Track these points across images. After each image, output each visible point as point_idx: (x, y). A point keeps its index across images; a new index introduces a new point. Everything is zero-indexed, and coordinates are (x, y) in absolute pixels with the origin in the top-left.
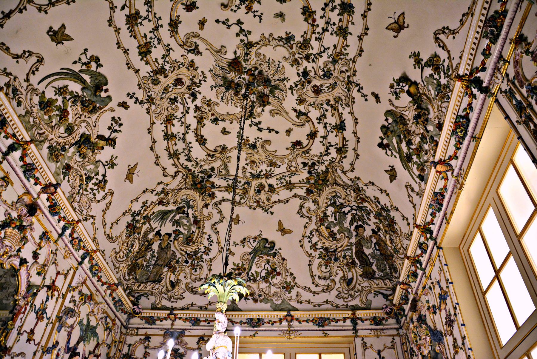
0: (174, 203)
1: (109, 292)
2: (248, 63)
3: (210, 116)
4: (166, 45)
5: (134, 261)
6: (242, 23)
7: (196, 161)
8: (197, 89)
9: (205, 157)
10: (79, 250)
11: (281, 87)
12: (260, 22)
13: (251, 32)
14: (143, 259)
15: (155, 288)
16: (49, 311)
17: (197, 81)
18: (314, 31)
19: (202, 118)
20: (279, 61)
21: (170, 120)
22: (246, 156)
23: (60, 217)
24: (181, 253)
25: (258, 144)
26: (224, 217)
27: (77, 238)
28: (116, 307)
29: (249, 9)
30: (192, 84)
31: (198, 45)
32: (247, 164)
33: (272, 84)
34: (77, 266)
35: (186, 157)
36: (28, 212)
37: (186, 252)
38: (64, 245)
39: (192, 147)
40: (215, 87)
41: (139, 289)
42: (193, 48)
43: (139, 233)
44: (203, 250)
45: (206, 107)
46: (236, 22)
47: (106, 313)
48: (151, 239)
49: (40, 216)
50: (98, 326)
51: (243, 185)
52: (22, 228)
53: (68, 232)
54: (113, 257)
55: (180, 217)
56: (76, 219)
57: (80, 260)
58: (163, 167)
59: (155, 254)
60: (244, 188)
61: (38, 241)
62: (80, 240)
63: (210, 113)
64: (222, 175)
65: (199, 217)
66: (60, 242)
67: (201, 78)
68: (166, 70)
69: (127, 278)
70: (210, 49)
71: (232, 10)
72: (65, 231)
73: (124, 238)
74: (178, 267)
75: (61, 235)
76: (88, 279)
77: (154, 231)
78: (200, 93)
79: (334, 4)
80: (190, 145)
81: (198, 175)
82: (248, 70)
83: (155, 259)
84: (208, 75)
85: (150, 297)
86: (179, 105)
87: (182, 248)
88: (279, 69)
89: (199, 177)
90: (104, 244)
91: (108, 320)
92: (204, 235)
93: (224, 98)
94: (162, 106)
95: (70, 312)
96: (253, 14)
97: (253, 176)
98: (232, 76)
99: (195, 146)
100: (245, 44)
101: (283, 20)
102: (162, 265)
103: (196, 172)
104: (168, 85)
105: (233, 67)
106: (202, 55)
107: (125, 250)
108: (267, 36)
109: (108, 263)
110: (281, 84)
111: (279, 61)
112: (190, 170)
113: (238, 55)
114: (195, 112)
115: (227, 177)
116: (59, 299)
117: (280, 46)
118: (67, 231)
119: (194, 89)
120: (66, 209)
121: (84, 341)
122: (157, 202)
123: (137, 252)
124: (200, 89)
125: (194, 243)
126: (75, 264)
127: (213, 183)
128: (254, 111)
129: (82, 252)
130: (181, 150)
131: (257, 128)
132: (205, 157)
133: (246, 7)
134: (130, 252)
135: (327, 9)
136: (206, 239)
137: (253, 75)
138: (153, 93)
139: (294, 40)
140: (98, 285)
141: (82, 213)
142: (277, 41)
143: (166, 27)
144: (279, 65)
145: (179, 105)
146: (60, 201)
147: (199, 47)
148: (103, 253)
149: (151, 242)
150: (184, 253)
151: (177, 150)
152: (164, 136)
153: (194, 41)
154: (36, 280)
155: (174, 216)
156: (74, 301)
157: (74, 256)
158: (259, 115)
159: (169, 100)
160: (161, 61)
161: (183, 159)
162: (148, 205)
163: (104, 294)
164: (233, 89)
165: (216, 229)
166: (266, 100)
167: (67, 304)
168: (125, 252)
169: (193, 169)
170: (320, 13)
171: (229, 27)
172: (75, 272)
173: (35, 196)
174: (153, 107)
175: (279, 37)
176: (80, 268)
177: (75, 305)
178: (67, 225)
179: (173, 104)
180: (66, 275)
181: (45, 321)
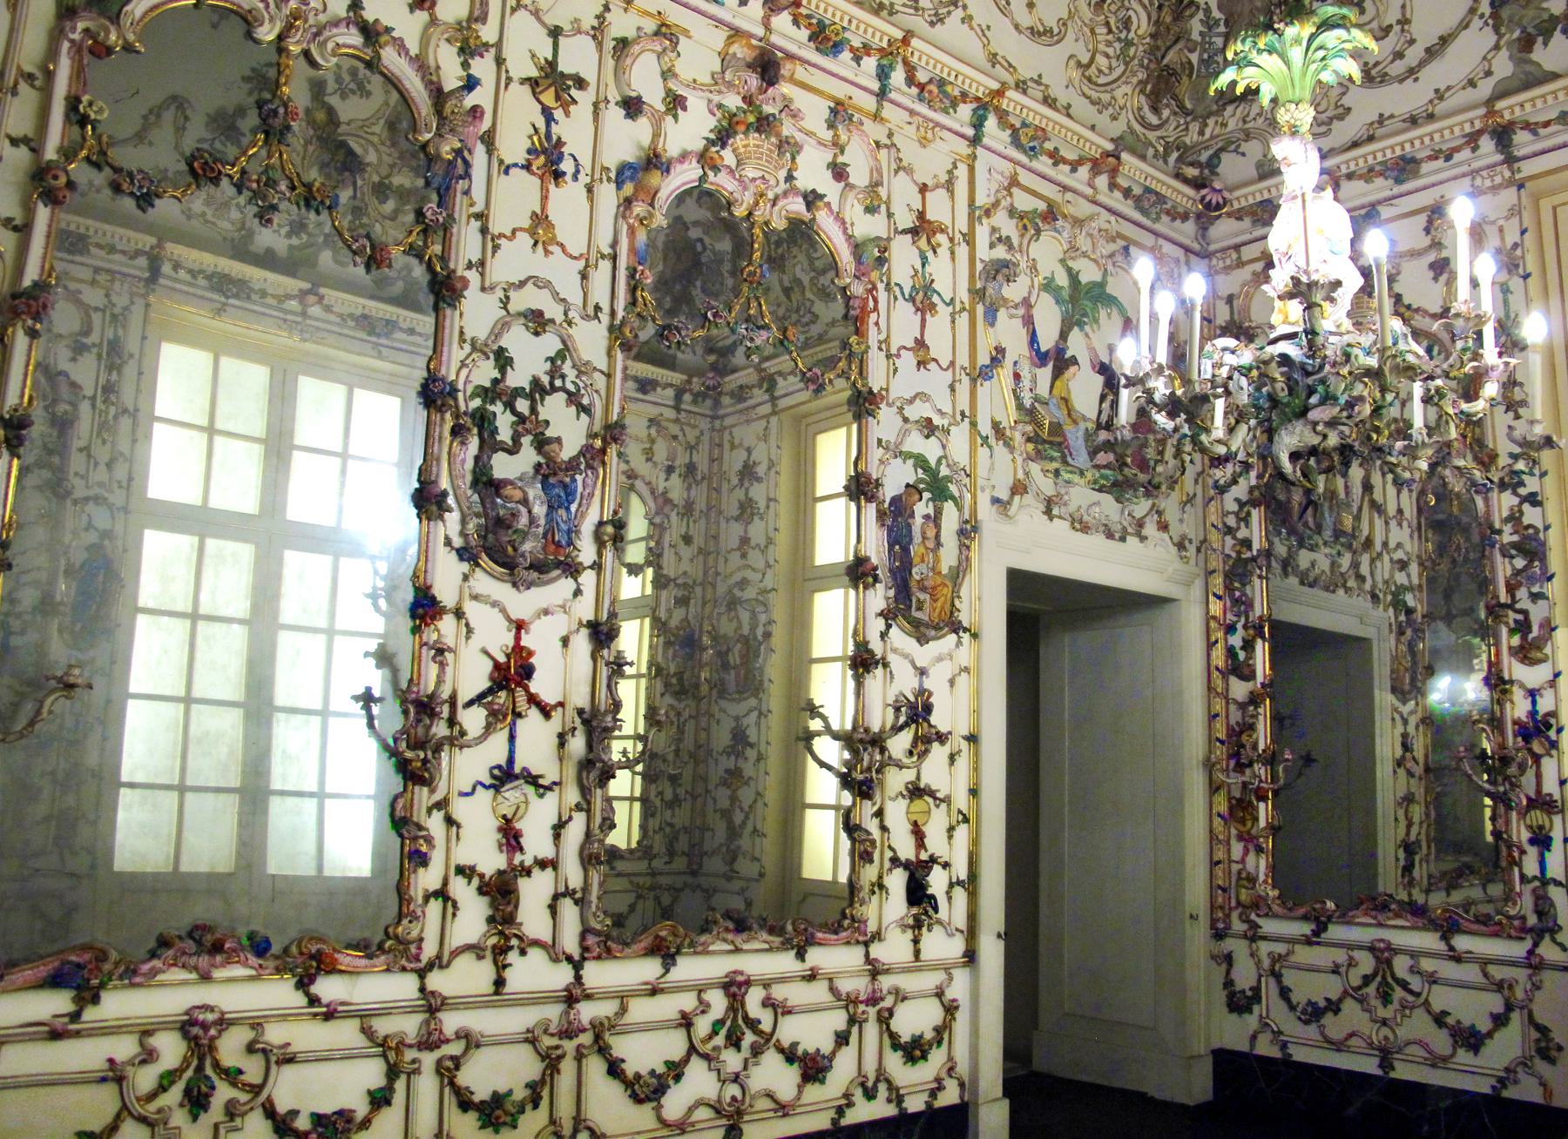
1: (1102, 181)
5: (1152, 66)
10: (954, 105)
15: (1252, 115)
16: (943, 285)
23: (852, 50)
27: (931, 81)
28: (1144, 212)
34: (969, 151)
36: (763, 79)
38: (905, 115)
41: (1207, 135)
47: (1119, 235)
49: (801, 73)
50: (1110, 279)
52: (764, 124)
53: (898, 77)
54: (1076, 83)
56: (899, 35)
57: (970, 132)
59: (1216, 14)
61: (828, 135)
62: (942, 83)
66: (889, 111)
69: (1154, 120)
72: (887, 77)
73: (1087, 13)
75: (882, 94)
76: (1019, 169)
83: (1222, 29)
85: (1244, 147)
90: (1029, 58)
95: (1001, 270)
107: (1109, 44)
109: (1067, 111)
116: (957, 249)
118: (893, 74)
120: (854, 22)
121: (1080, 324)
123: (1152, 36)
126: (963, 148)
129: (965, 111)
134: (1129, 43)
140: (1062, 173)
141: (916, 9)
146: (826, 11)
148: (1038, 83)
154: (868, 226)
156: (1007, 241)
157: (950, 130)
163: (1089, 191)
167: (983, 252)
168: (1110, 51)
172: (971, 169)
173: (760, 31)
176: (980, 151)
177: (1011, 247)
178: (885, 62)
180: (949, 186)
181: (943, 311)
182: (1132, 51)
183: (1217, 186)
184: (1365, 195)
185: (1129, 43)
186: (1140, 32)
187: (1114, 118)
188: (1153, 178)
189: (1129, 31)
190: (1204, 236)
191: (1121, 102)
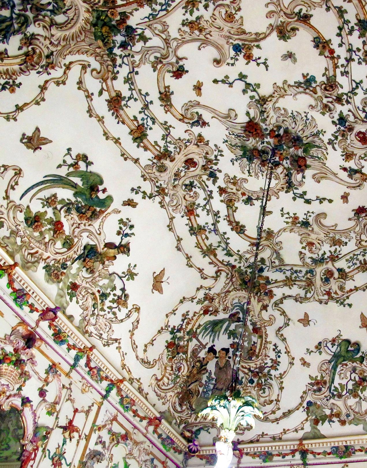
0: (224, 310)
1: (151, 428)
2: (267, 123)
3: (241, 196)
4: (163, 123)
5: (184, 388)
6: (245, 77)
7: (238, 254)
8: (215, 167)
9: (249, 248)
11: (317, 144)
12: (267, 70)
13: (259, 85)
14: (195, 384)
17: (213, 157)
18: (336, 64)
19: (230, 201)
20: (305, 112)
21: (192, 210)
22: (300, 237)
24: (243, 371)
25: (311, 220)
26: (289, 319)
29: (249, 57)
30: (207, 162)
31: (201, 115)
32: (303, 248)
33: (305, 142)
35: (225, 252)
37: (249, 369)
39: (228, 238)
40: (236, 160)
42: (196, 119)
43: (186, 353)
44: (270, 364)
45: (232, 186)
46: (238, 78)
47: (151, 453)
48: (204, 358)
51: (305, 275)
54: (153, 386)
55: (236, 326)
58: (199, 269)
59: (213, 376)
60: (307, 278)
63: (240, 193)
64: (276, 266)
65: (258, 323)
67: (216, 153)
68: (172, 152)
69: (179, 409)
70: (216, 116)
71: (228, 64)
73: (165, 360)
74: (241, 389)
77: (205, 348)
78: (220, 171)
79: (350, 25)
80: (226, 236)
81: (246, 272)
82: (270, 131)
83: (214, 382)
84: (224, 147)
86: (197, 190)
87: (244, 364)
88: (308, 122)
89: (248, 273)
91: (156, 462)
92: (268, 346)
93: (251, 171)
94: (177, 196)
96: (255, 63)
97: (316, 261)
98: (252, 142)
99: (233, 236)
100: (256, 100)
101: (295, 60)
102: (222, 389)
103: (242, 268)
104: (179, 169)
105: (250, 132)
106: (209, 126)
107: (170, 374)
108: (280, 84)
110: (316, 139)
111: (305, 112)
112: (234, 267)
113: (252, 116)
114: (221, 195)
115: (283, 268)
117: (301, 93)
119: (211, 168)
122: (202, 312)
123: (188, 377)
124: (219, 166)
125: (257, 356)
127: (267, 278)
128: (293, 179)
130: (215, 244)
131: (303, 200)
132: (249, 248)
133: (244, 56)
134: (177, 377)
135: (343, 33)
136: (271, 349)
137: (279, 135)
138: (162, 183)
139: (315, 82)
142: (295, 88)
143: (157, 103)
144: (306, 116)
145: (197, 190)
147: (204, 117)
148: (138, 381)
149: (205, 362)
150: (246, 371)
151: (211, 245)
152: (189, 231)
153: (195, 110)
155: (228, 326)
158: (301, 184)
159: (184, 187)
160: (162, 143)
161: (221, 255)
162: (190, 316)
163: (145, 431)
164: (257, 158)
165: (282, 335)
166: (303, 164)
168: (170, 377)
169: (238, 266)
170: (335, 41)
171: (231, 85)
174: (167, 199)
175: (295, 83)
179: (191, 190)
182: (178, 380)
183: (196, 443)
184: (251, 463)
185: (177, 377)
186: (183, 374)
187: (164, 404)
188: (172, 433)
189: (179, 372)
190: (185, 463)
191: (169, 398)
